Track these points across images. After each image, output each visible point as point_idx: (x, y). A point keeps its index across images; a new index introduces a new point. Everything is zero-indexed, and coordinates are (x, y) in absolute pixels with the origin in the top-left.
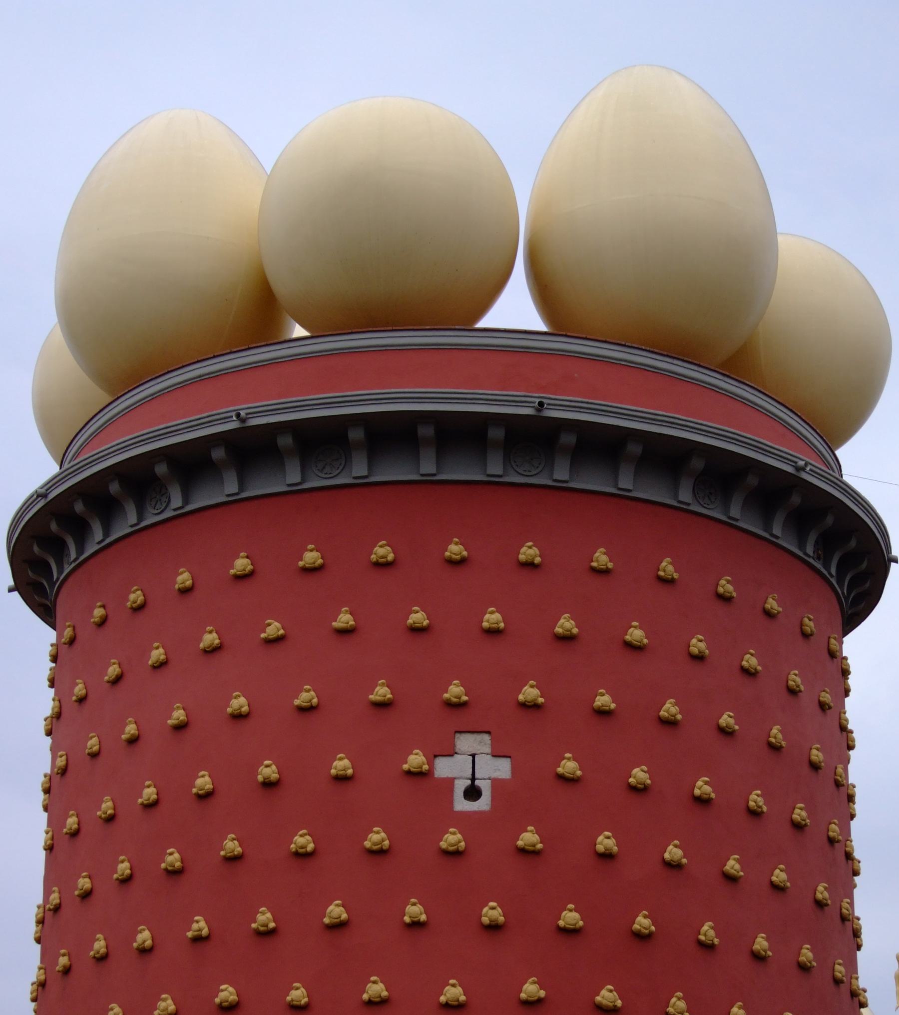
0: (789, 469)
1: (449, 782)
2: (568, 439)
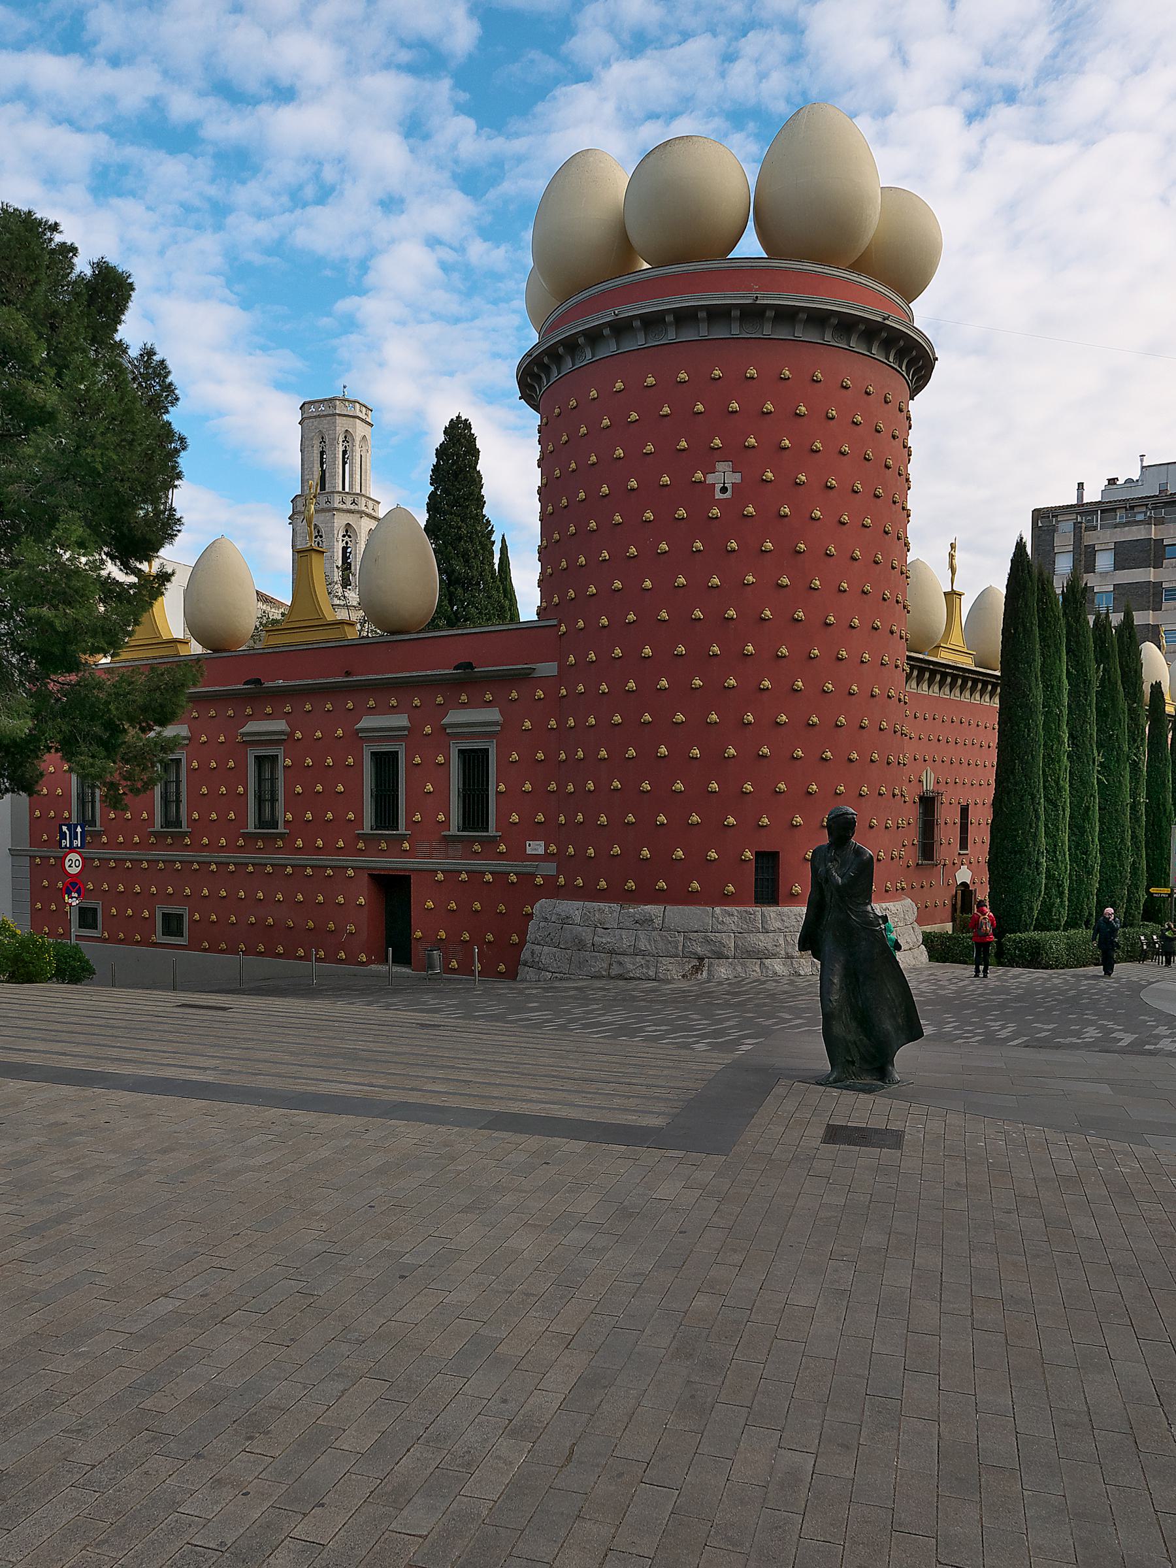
0: (880, 320)
2: (770, 314)
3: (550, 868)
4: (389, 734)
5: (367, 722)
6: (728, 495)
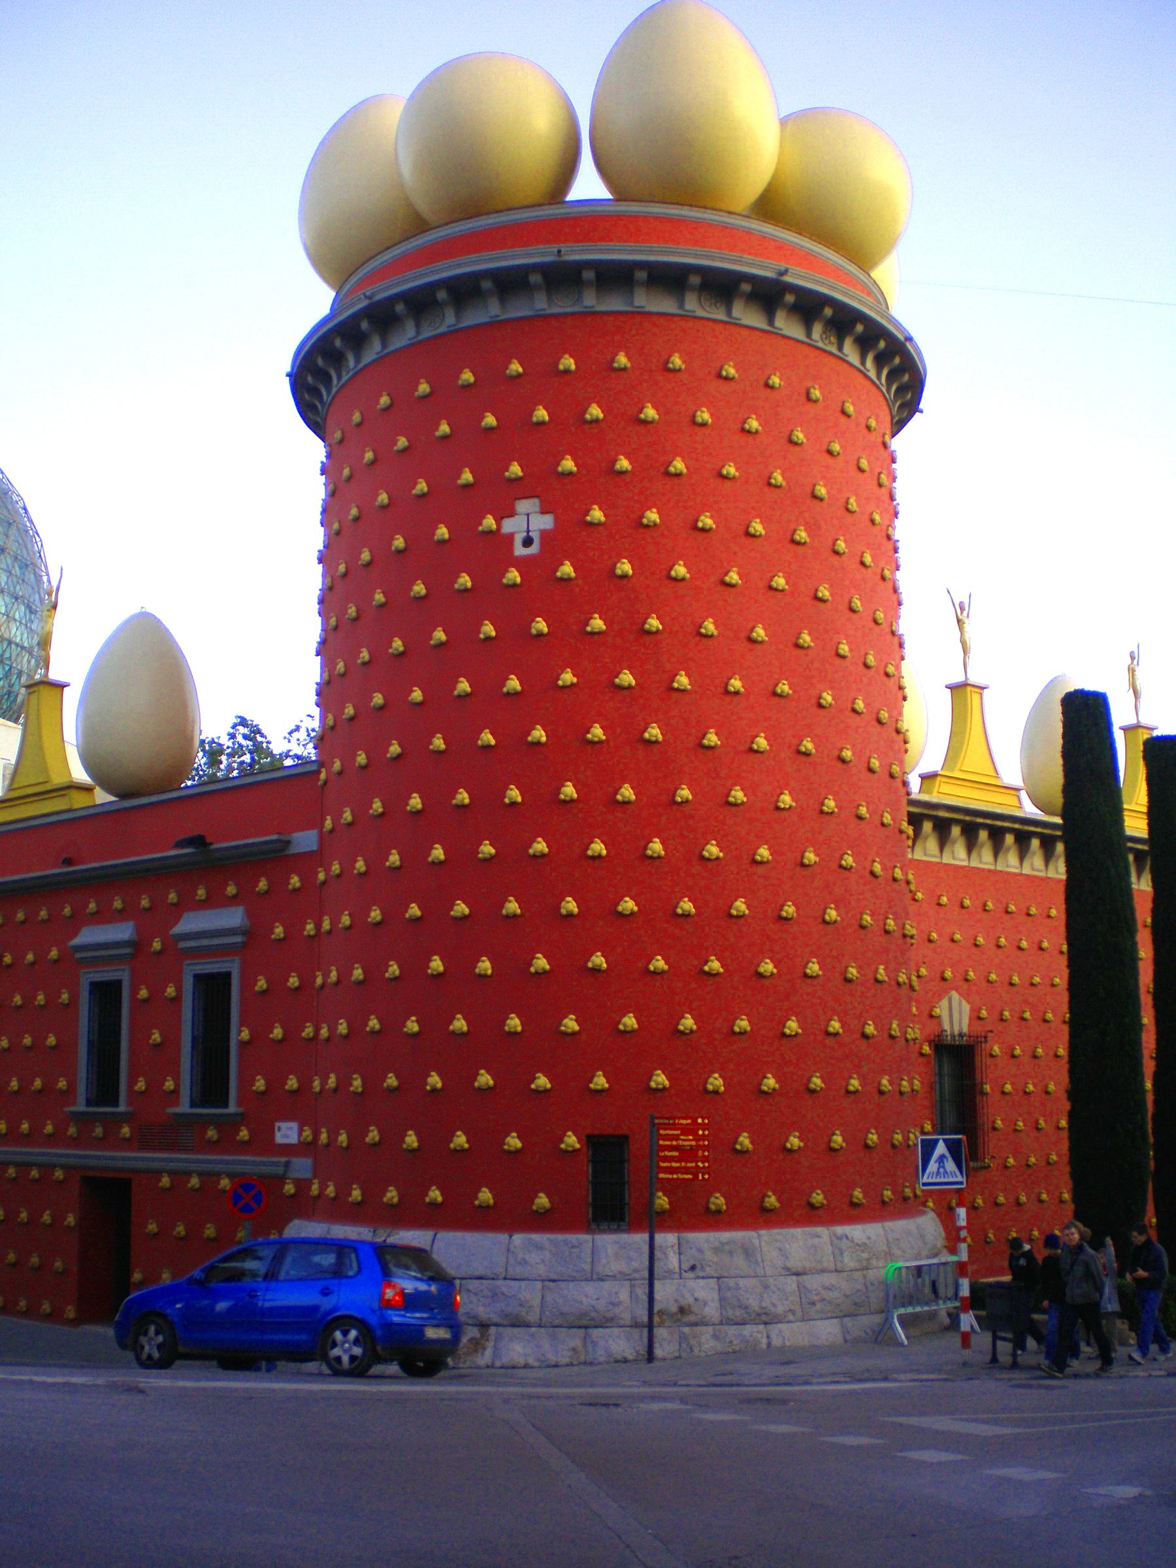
1: (511, 537)
3: (302, 1167)
4: (102, 954)
5: (89, 935)
6: (534, 549)
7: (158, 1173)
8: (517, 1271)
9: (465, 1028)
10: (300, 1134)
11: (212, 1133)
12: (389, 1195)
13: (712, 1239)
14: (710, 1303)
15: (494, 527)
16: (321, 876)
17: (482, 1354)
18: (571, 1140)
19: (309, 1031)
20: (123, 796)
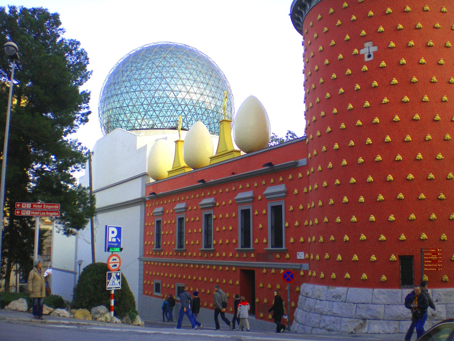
1: (363, 55)
3: (306, 266)
4: (244, 201)
6: (371, 58)
7: (262, 268)
8: (375, 301)
9: (356, 220)
10: (305, 256)
11: (278, 256)
12: (333, 275)
13: (444, 291)
14: (443, 313)
15: (358, 52)
16: (308, 173)
17: (364, 329)
18: (393, 257)
19: (306, 223)
20: (248, 153)
